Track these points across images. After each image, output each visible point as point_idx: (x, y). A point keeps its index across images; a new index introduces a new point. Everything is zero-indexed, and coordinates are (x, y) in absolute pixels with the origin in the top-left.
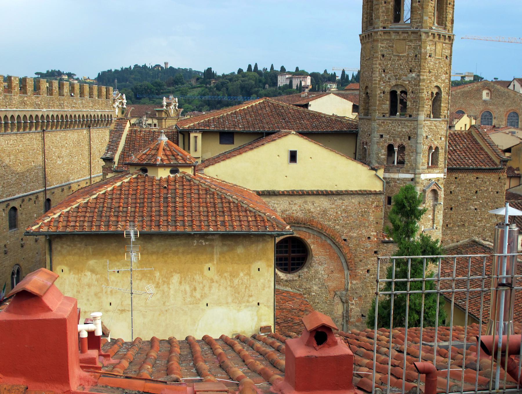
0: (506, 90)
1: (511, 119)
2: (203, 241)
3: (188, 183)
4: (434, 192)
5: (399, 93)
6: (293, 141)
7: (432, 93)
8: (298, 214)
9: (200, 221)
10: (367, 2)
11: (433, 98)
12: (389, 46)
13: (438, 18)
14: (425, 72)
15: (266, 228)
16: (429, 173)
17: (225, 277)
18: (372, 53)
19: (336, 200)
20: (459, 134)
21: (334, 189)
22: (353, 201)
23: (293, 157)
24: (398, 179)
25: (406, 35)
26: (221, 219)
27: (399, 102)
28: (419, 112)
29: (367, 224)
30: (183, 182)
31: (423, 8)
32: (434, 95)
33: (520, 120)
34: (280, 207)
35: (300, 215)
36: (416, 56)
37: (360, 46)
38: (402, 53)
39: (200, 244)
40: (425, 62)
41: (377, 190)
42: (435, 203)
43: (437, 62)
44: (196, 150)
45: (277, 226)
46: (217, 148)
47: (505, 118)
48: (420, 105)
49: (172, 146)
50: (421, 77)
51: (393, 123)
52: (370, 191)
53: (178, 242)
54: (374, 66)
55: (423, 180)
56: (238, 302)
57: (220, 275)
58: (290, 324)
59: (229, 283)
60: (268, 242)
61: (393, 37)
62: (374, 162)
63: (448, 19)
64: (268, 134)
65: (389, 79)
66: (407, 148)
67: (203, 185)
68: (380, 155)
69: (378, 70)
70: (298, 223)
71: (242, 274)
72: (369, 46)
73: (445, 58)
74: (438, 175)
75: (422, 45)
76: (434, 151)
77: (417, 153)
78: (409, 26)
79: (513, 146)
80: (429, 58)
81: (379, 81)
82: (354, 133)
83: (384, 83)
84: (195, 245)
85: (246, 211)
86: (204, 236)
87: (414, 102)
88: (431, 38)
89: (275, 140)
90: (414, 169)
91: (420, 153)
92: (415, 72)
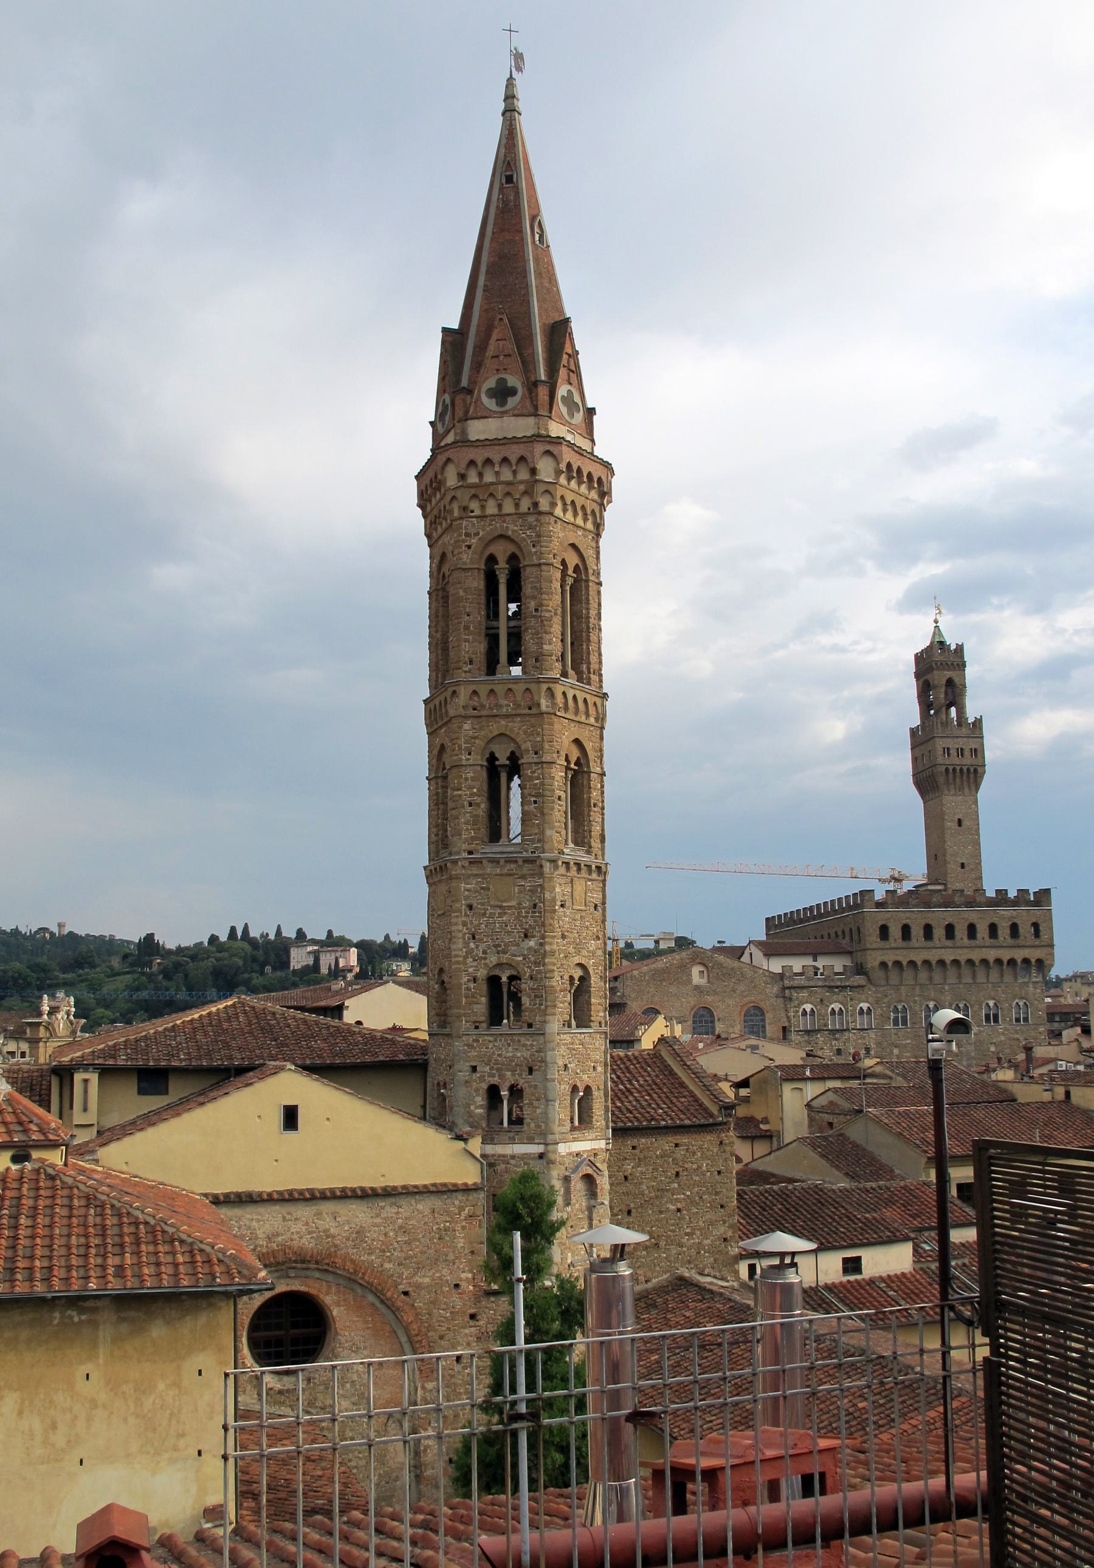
0: (736, 964)
1: (752, 1021)
2: (74, 1313)
3: (49, 1183)
4: (589, 1179)
5: (504, 979)
6: (290, 1085)
7: (571, 978)
8: (304, 1241)
9: (69, 1268)
10: (437, 804)
12: (482, 888)
13: (575, 831)
15: (214, 1278)
16: (575, 1140)
17: (124, 1393)
18: (449, 901)
19: (383, 1208)
20: (636, 1058)
21: (379, 1183)
22: (420, 1207)
23: (291, 1118)
24: (513, 1157)
25: (513, 866)
26: (117, 1261)
27: (503, 997)
29: (451, 1257)
30: (37, 1181)
31: (543, 814)
32: (577, 982)
33: (767, 1021)
34: (265, 1225)
35: (307, 1243)
36: (535, 906)
37: (426, 888)
38: (505, 901)
39: (67, 1321)
40: (552, 918)
41: (470, 1182)
42: (592, 1202)
43: (578, 917)
44: (85, 1110)
45: (239, 1272)
46: (131, 1102)
49: (19, 1103)
50: (547, 948)
51: (496, 1040)
52: (455, 1185)
53: (16, 1316)
54: (454, 928)
55: (563, 1157)
56: (152, 1451)
57: (111, 1390)
58: (282, 1495)
59: (132, 1408)
60: (220, 1308)
61: (488, 870)
62: (460, 1122)
64: (241, 1071)
65: (484, 952)
66: (527, 1092)
67: (81, 1186)
68: (472, 1107)
69: (460, 935)
70: (303, 1262)
71: (161, 1386)
72: (443, 888)
73: (592, 909)
74: (592, 1144)
75: (546, 885)
77: (548, 1101)
78: (518, 849)
79: (752, 1076)
81: (465, 958)
82: (419, 1065)
83: (475, 960)
84: (56, 1322)
85: (172, 1241)
86: (76, 1301)
87: (536, 996)
88: (562, 870)
89: (251, 1084)
90: (543, 1135)
91: (554, 1101)
92: (534, 937)
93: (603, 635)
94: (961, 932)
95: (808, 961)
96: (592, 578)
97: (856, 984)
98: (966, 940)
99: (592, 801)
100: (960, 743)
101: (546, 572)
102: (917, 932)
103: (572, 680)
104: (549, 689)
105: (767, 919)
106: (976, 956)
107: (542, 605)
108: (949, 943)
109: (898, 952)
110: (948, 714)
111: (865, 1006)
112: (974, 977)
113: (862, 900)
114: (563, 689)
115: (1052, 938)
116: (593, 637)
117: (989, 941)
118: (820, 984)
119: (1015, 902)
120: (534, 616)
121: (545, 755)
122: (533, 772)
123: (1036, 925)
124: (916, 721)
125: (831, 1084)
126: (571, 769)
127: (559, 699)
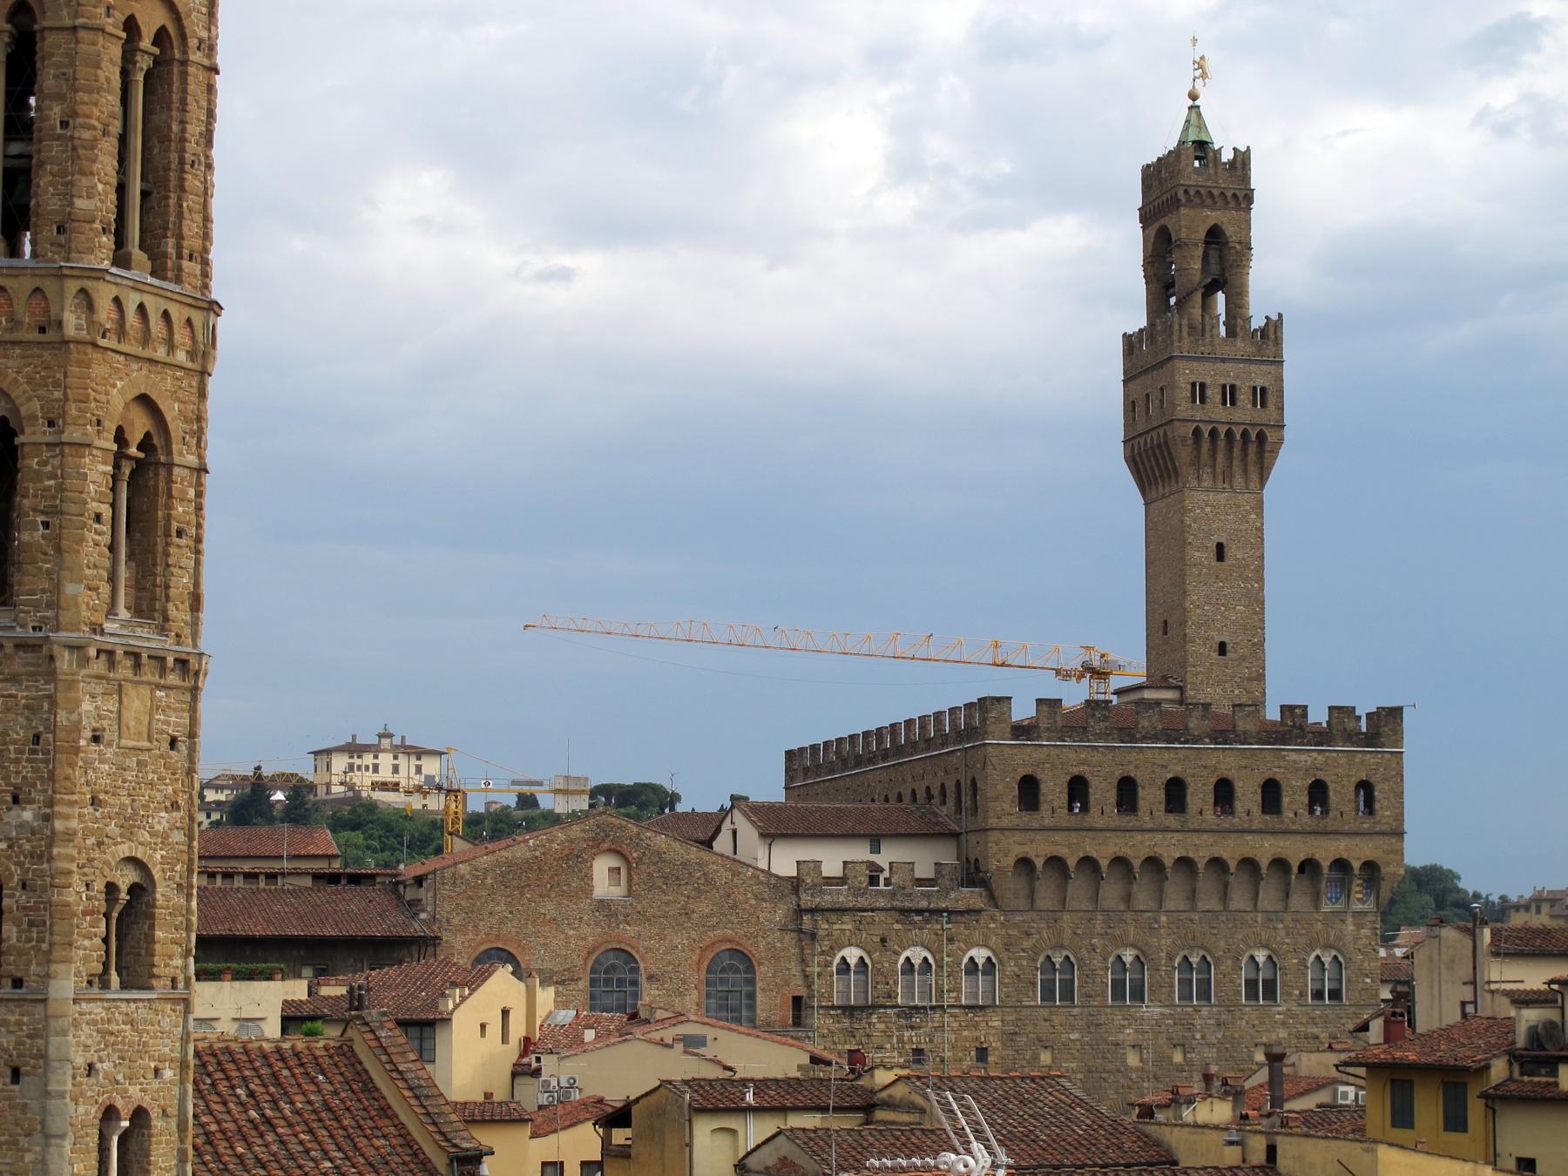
0: (694, 854)
1: (722, 981)
7: (111, 888)
11: (118, 908)
14: (71, 804)
20: (297, 1055)
28: (54, 967)
31: (59, 550)
32: (124, 896)
33: (759, 984)
36: (37, 738)
47: (696, 977)
48: (57, 938)
50: (59, 825)
63: (173, 592)
73: (166, 745)
75: (60, 696)
76: (125, 1124)
77: (47, 1136)
79: (637, 1100)
80: (93, 747)
87: (31, 924)
88: (99, 667)
91: (62, 1136)
93: (218, 177)
94: (1199, 796)
95: (859, 852)
96: (195, 56)
97: (961, 906)
98: (1209, 815)
99: (175, 525)
100: (1230, 373)
101: (88, 45)
102: (1103, 792)
103: (140, 272)
104: (83, 290)
105: (790, 755)
106: (1231, 850)
107: (75, 114)
108: (1173, 820)
109: (1058, 837)
110: (1207, 305)
111: (980, 955)
112: (1224, 896)
113: (984, 720)
114: (114, 291)
115: (1399, 817)
116: (192, 182)
117: (1259, 819)
118: (882, 903)
119: (1322, 736)
120: (59, 137)
121: (69, 429)
122: (45, 463)
123: (1365, 787)
124: (1137, 320)
125: (797, 1121)
126: (129, 458)
127: (105, 313)
